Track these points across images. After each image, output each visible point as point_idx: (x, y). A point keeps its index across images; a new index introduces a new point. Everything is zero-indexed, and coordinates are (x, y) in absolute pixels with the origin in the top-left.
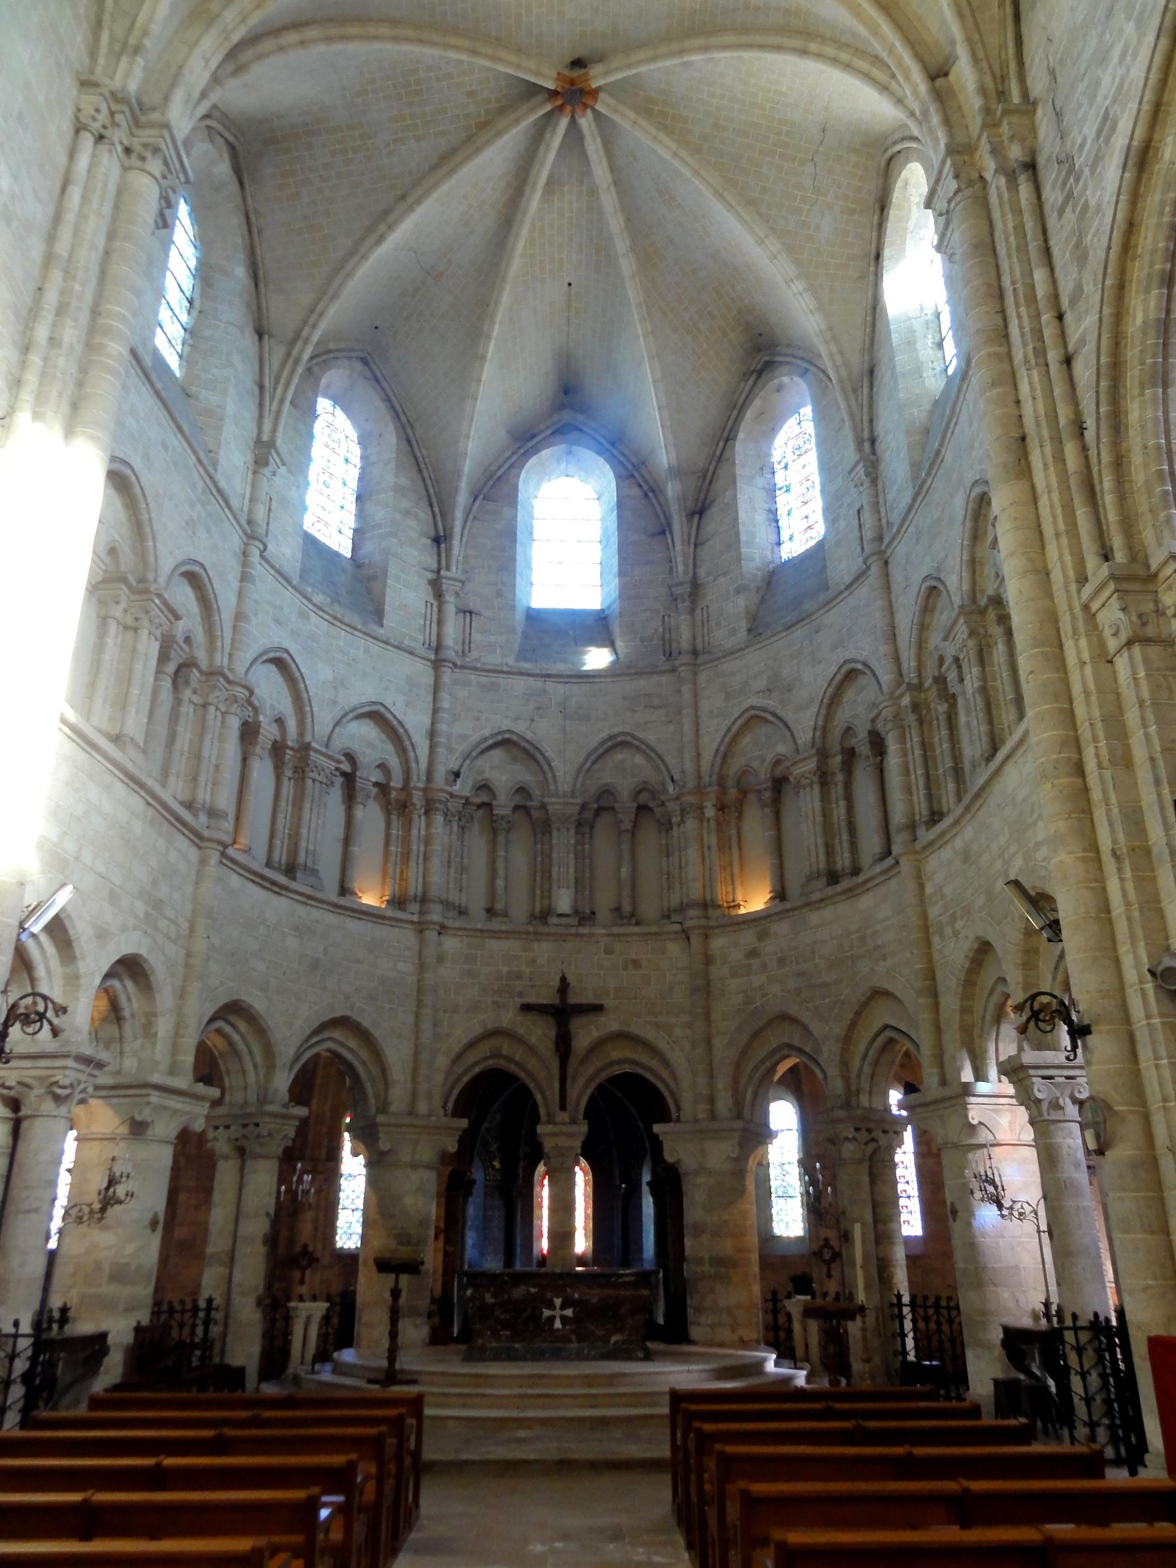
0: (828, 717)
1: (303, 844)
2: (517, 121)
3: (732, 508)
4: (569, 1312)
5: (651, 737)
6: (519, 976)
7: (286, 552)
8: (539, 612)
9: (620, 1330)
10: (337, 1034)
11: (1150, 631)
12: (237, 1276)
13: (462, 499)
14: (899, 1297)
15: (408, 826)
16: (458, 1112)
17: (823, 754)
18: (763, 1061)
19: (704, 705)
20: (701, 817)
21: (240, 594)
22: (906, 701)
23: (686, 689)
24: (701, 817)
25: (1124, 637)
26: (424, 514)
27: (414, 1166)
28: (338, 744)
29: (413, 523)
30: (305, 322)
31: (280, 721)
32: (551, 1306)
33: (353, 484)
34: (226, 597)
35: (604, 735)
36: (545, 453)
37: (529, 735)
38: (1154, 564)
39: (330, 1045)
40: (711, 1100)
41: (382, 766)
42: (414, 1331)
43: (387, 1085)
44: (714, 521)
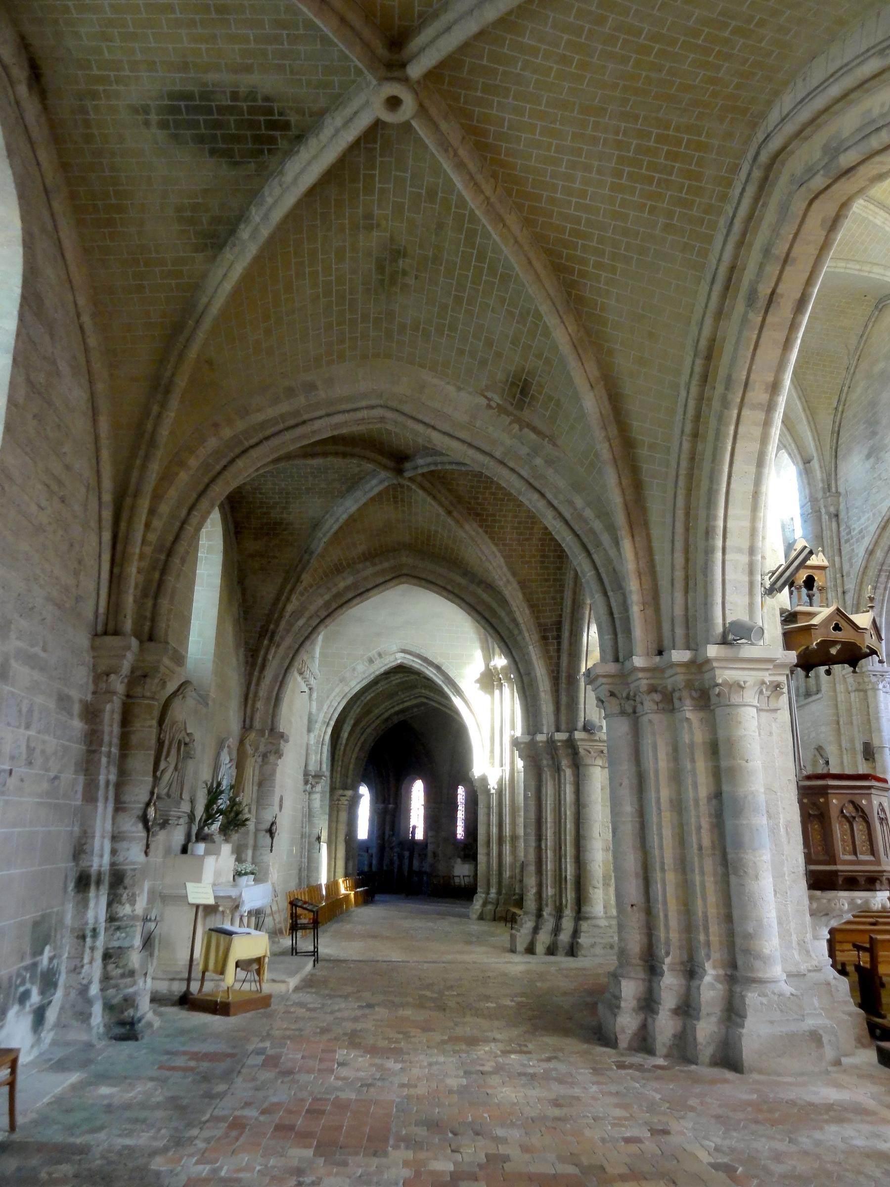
11: (861, 687)
25: (854, 688)
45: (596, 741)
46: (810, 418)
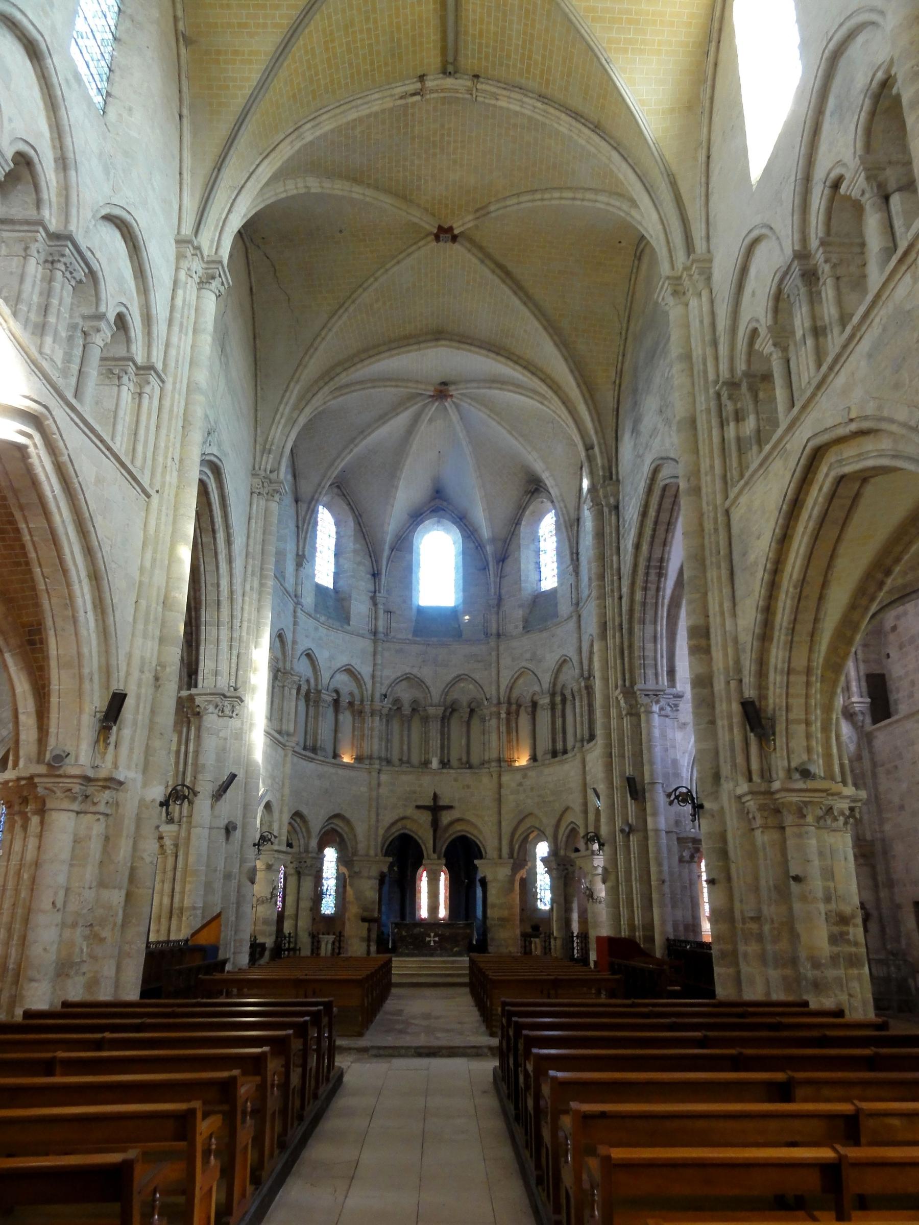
0: (556, 678)
1: (319, 737)
2: (416, 404)
3: (518, 561)
4: (437, 939)
5: (477, 677)
6: (415, 792)
7: (308, 600)
8: (423, 608)
9: (457, 946)
10: (336, 821)
11: (634, 711)
12: (300, 924)
13: (386, 553)
14: (573, 933)
15: (363, 721)
16: (387, 854)
17: (553, 695)
18: (523, 833)
19: (502, 662)
20: (499, 718)
21: (294, 632)
22: (583, 684)
23: (494, 654)
24: (499, 718)
26: (367, 562)
27: (369, 878)
28: (332, 687)
29: (362, 568)
30: (316, 492)
31: (308, 681)
33: (333, 548)
34: (289, 637)
35: (455, 674)
36: (427, 522)
37: (419, 675)
38: (635, 688)
39: (332, 826)
40: (500, 850)
41: (351, 694)
42: (373, 948)
43: (357, 843)
44: (509, 566)
45: (60, 776)
46: (587, 395)
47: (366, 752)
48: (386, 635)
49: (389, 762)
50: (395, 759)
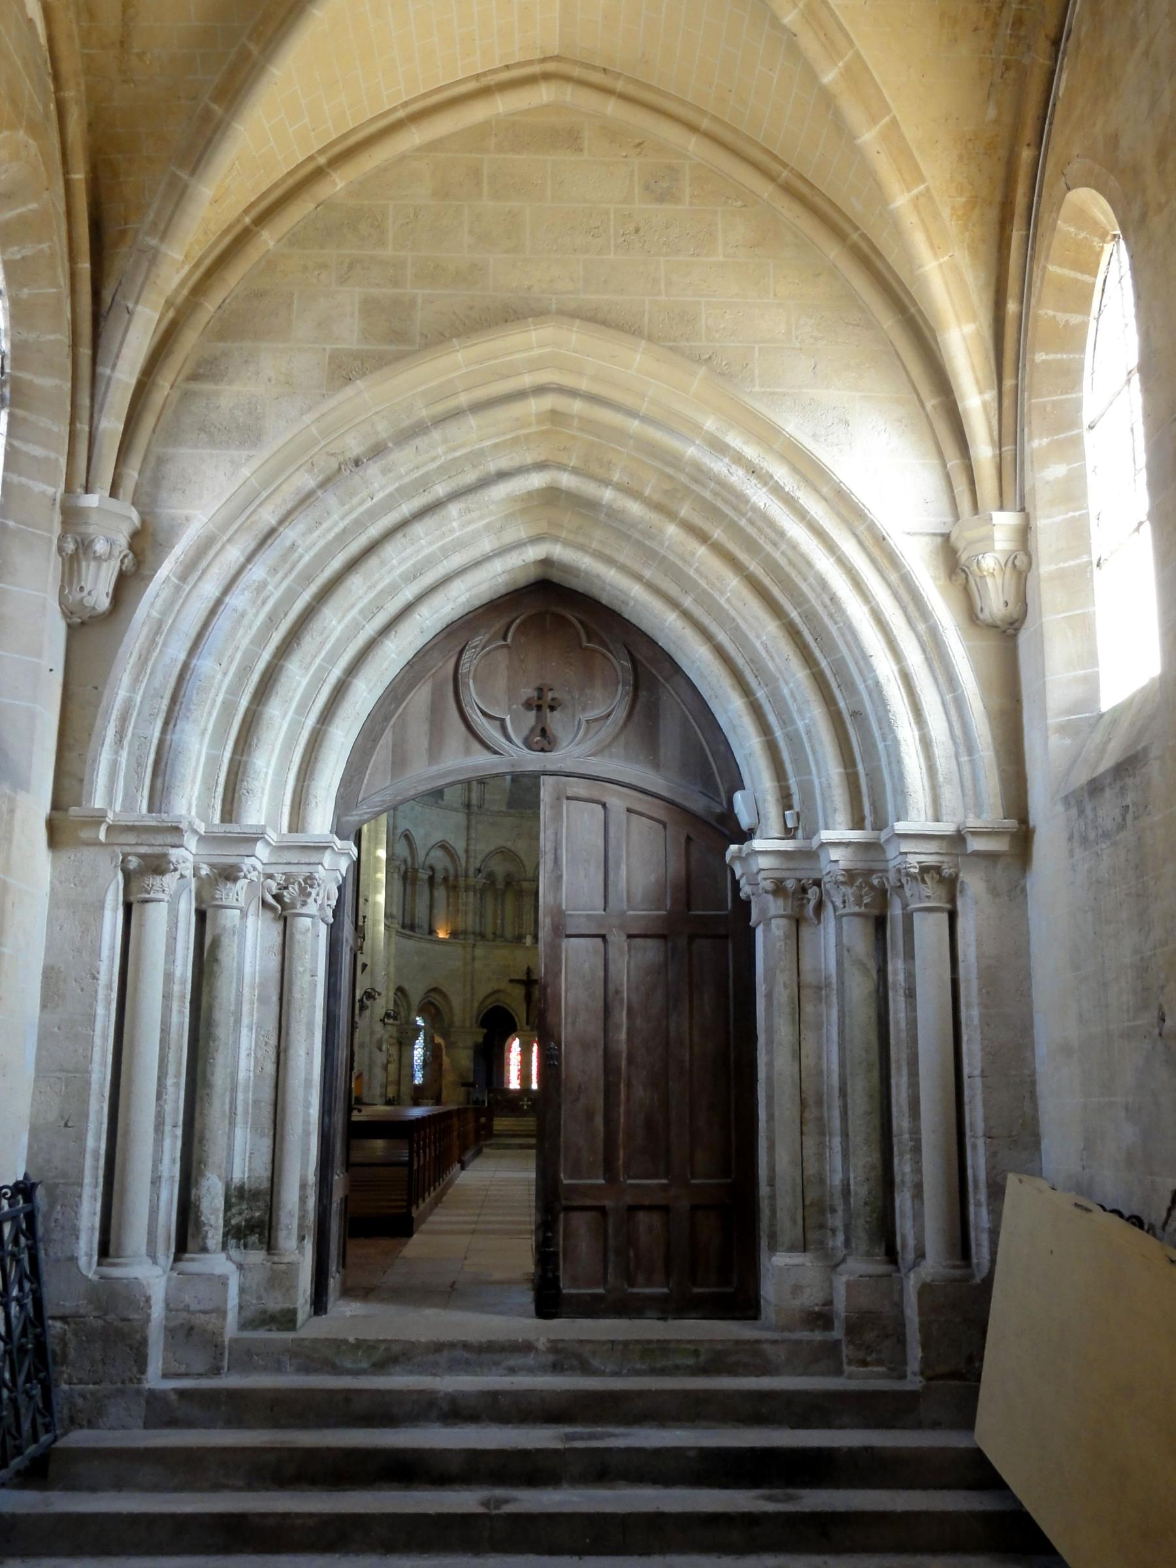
10: (432, 994)
28: (427, 863)
31: (405, 861)
32: (523, 1101)
37: (513, 849)
39: (430, 999)
47: (461, 926)
48: (480, 807)
49: (482, 936)
50: (489, 931)
